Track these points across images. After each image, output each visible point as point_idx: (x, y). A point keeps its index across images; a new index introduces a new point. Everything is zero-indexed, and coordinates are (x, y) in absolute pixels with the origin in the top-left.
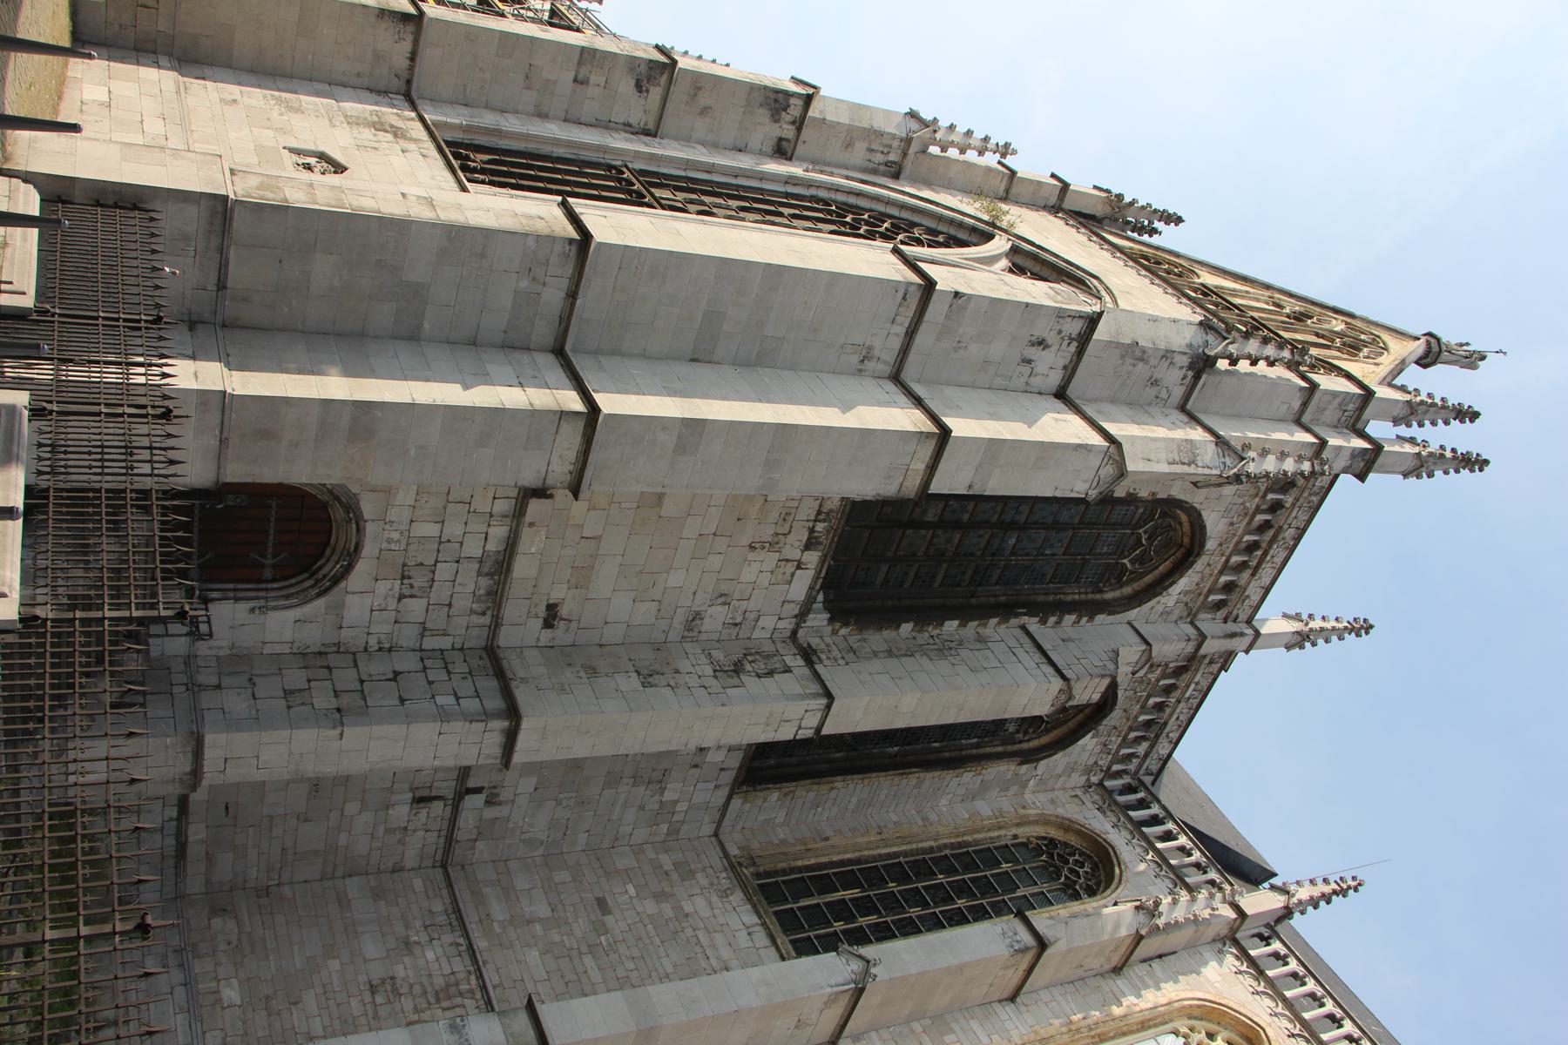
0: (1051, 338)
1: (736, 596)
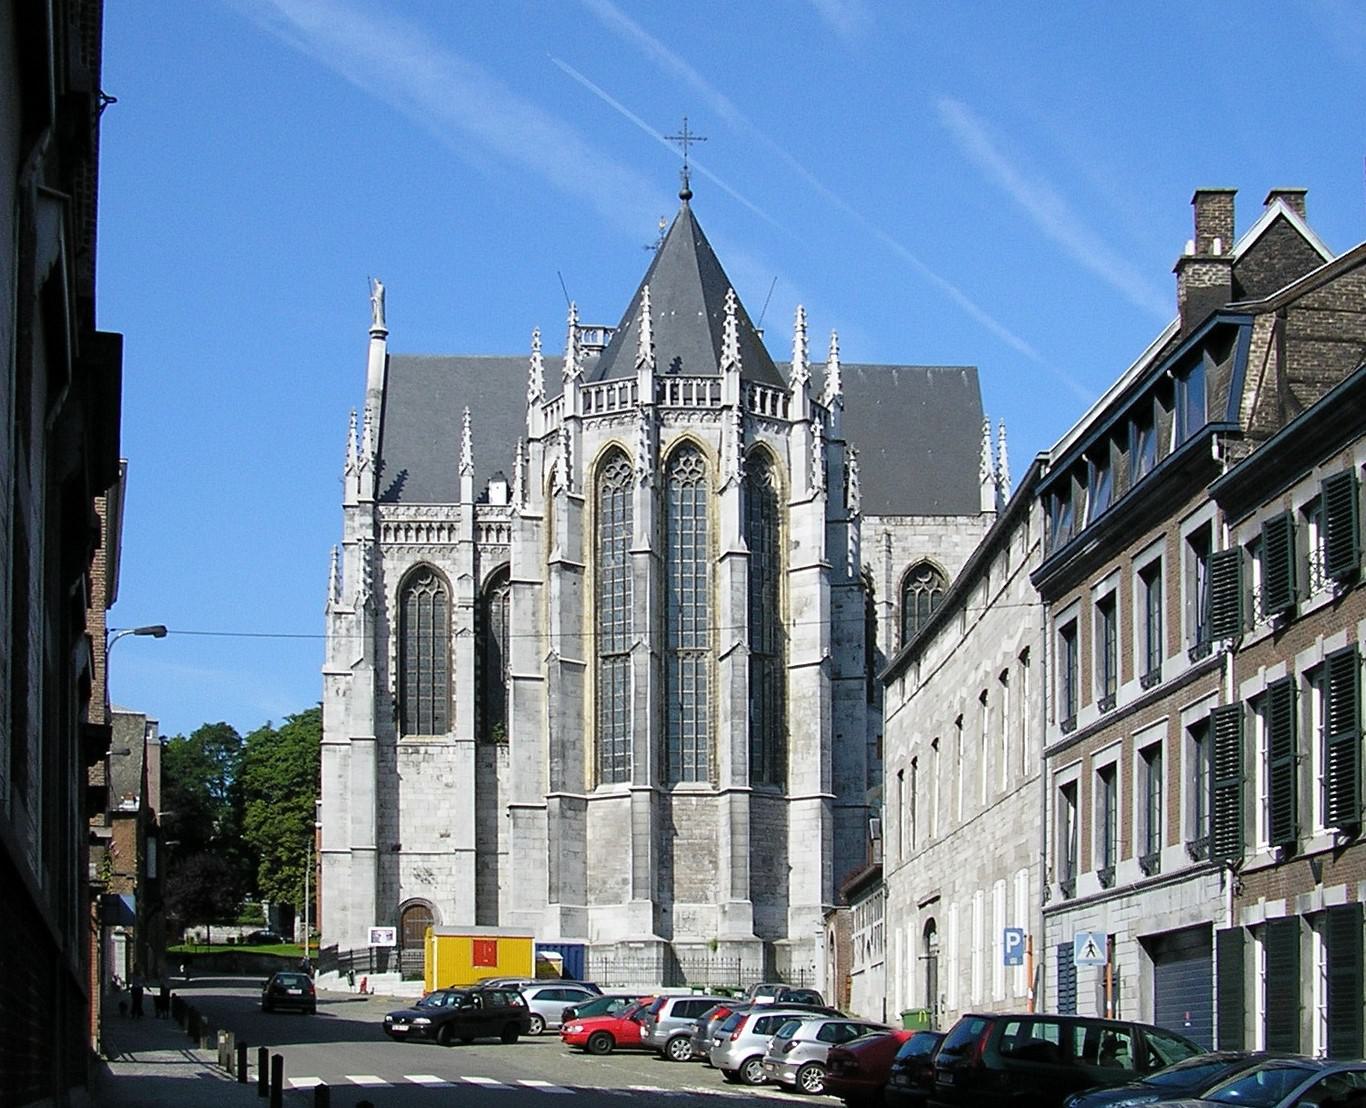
0: (335, 688)
1: (439, 773)
